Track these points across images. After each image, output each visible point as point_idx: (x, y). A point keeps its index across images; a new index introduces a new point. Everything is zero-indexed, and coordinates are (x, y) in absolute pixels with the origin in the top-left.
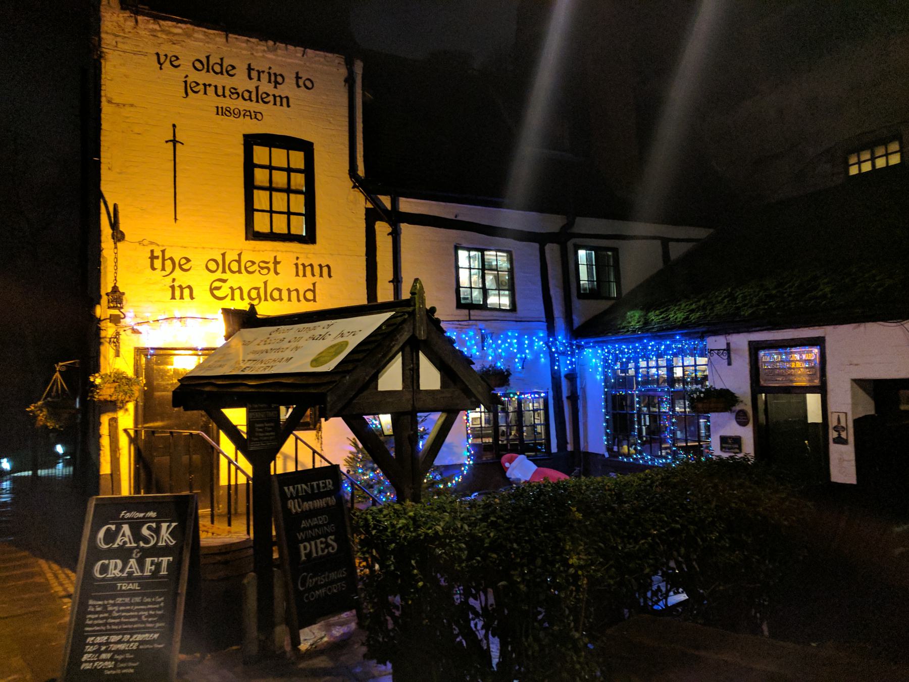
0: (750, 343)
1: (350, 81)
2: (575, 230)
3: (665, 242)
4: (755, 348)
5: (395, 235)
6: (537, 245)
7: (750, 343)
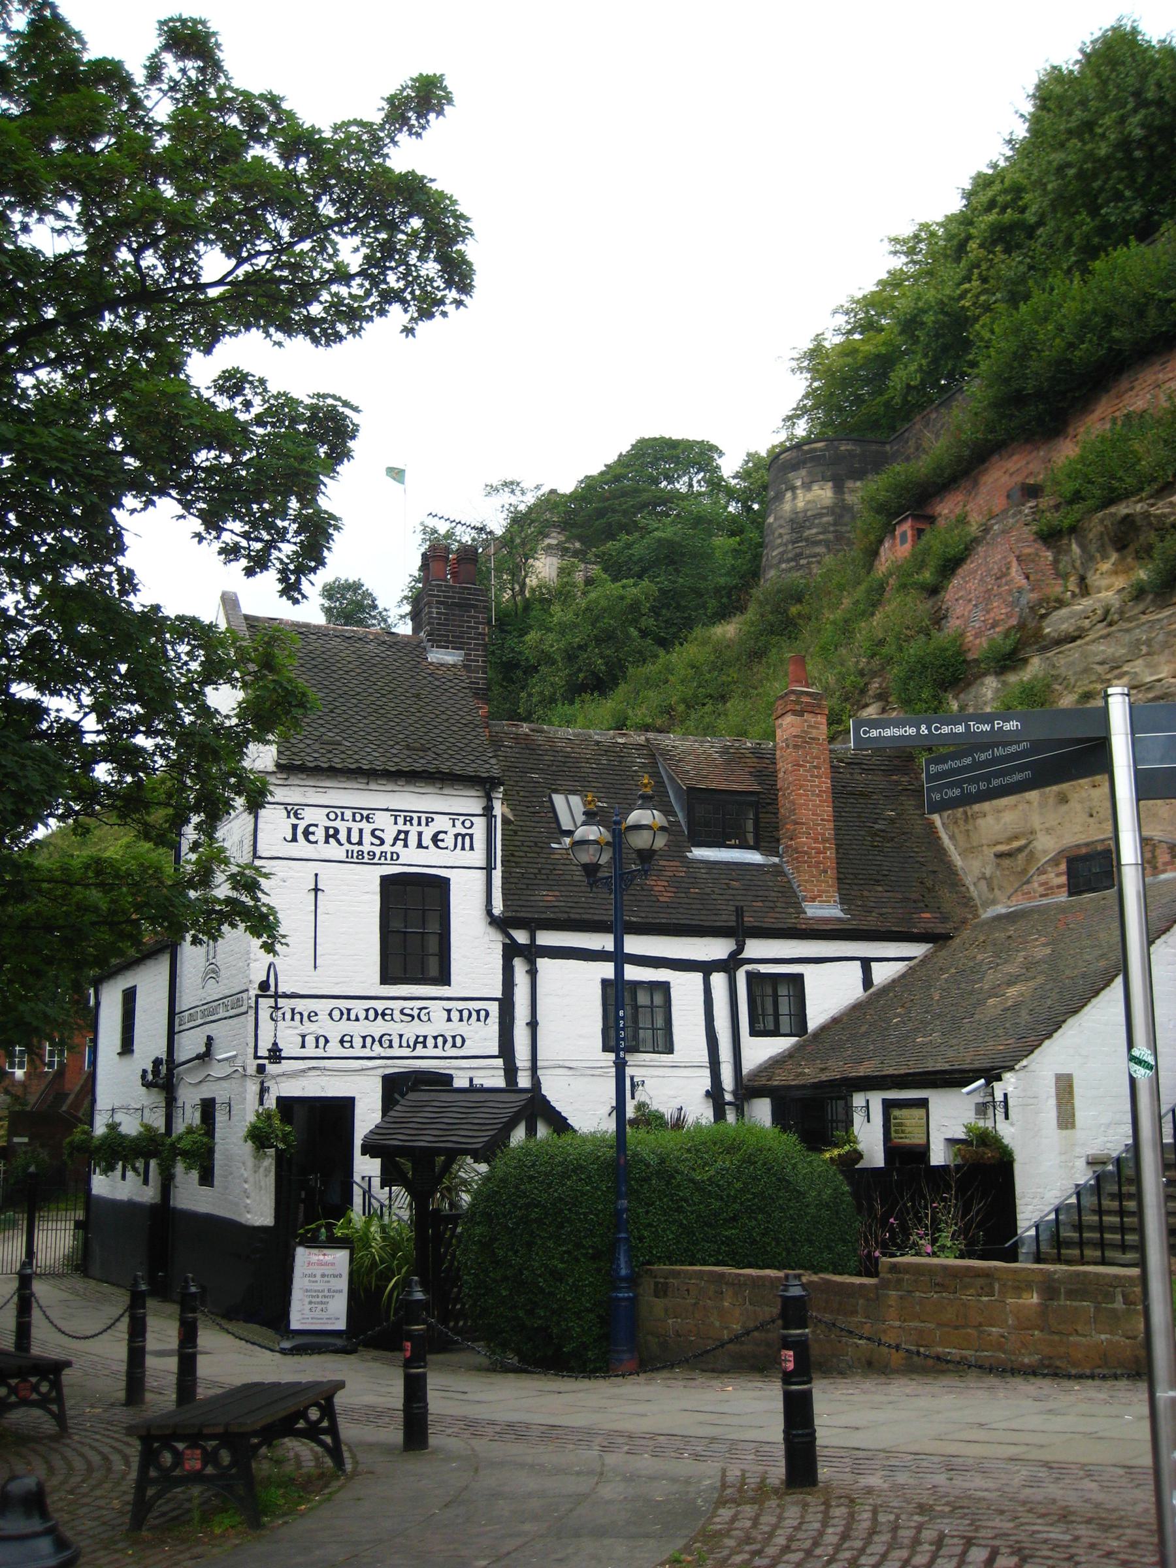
0: (884, 1100)
1: (488, 812)
2: (747, 954)
3: (866, 963)
4: (888, 1105)
5: (533, 973)
6: (698, 977)
7: (884, 1100)
